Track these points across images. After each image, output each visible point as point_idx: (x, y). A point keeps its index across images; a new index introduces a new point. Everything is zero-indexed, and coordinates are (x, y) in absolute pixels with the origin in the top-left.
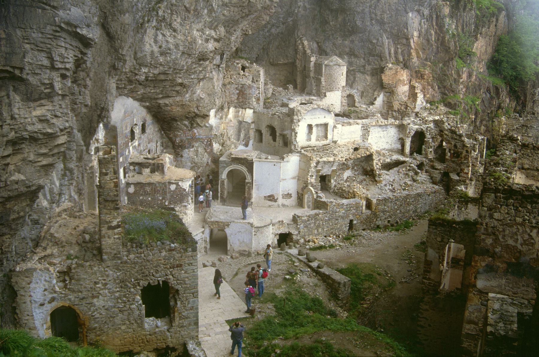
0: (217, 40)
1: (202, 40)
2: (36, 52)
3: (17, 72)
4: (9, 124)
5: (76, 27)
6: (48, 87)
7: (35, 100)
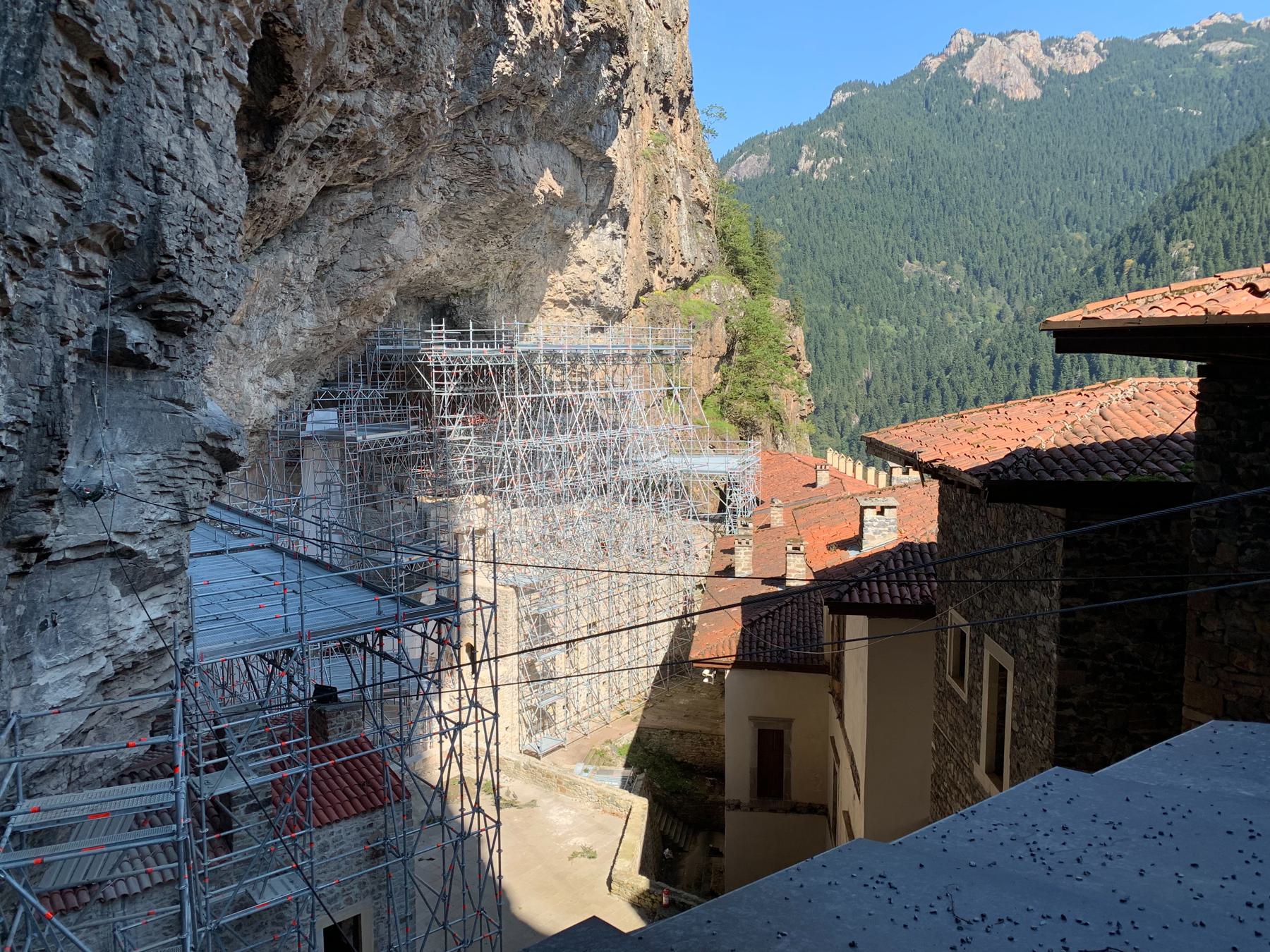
0: (283, 397)
1: (259, 398)
2: (158, 497)
3: (127, 543)
4: (105, 649)
5: (225, 439)
6: (170, 559)
7: (144, 589)
